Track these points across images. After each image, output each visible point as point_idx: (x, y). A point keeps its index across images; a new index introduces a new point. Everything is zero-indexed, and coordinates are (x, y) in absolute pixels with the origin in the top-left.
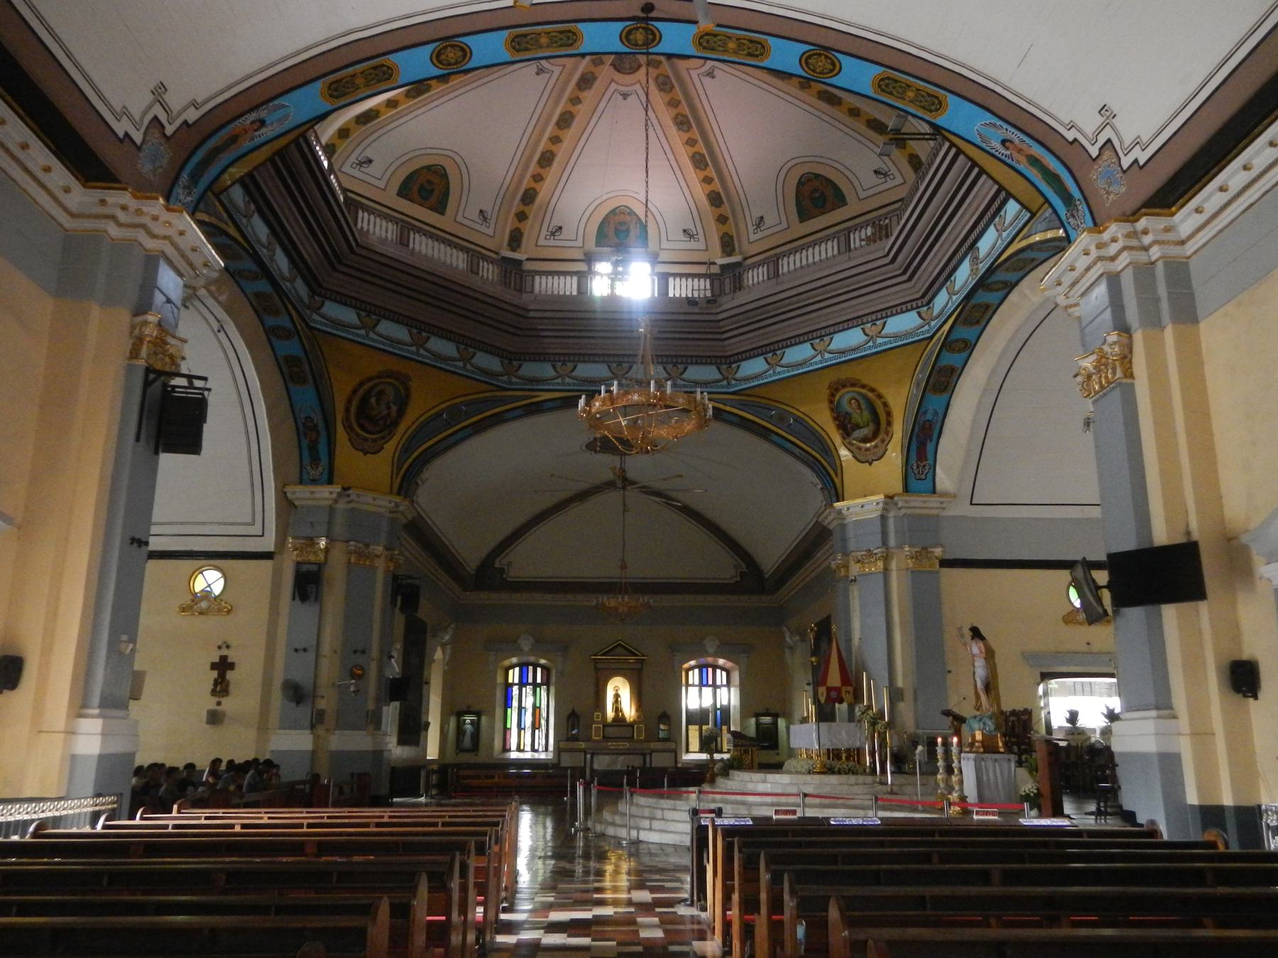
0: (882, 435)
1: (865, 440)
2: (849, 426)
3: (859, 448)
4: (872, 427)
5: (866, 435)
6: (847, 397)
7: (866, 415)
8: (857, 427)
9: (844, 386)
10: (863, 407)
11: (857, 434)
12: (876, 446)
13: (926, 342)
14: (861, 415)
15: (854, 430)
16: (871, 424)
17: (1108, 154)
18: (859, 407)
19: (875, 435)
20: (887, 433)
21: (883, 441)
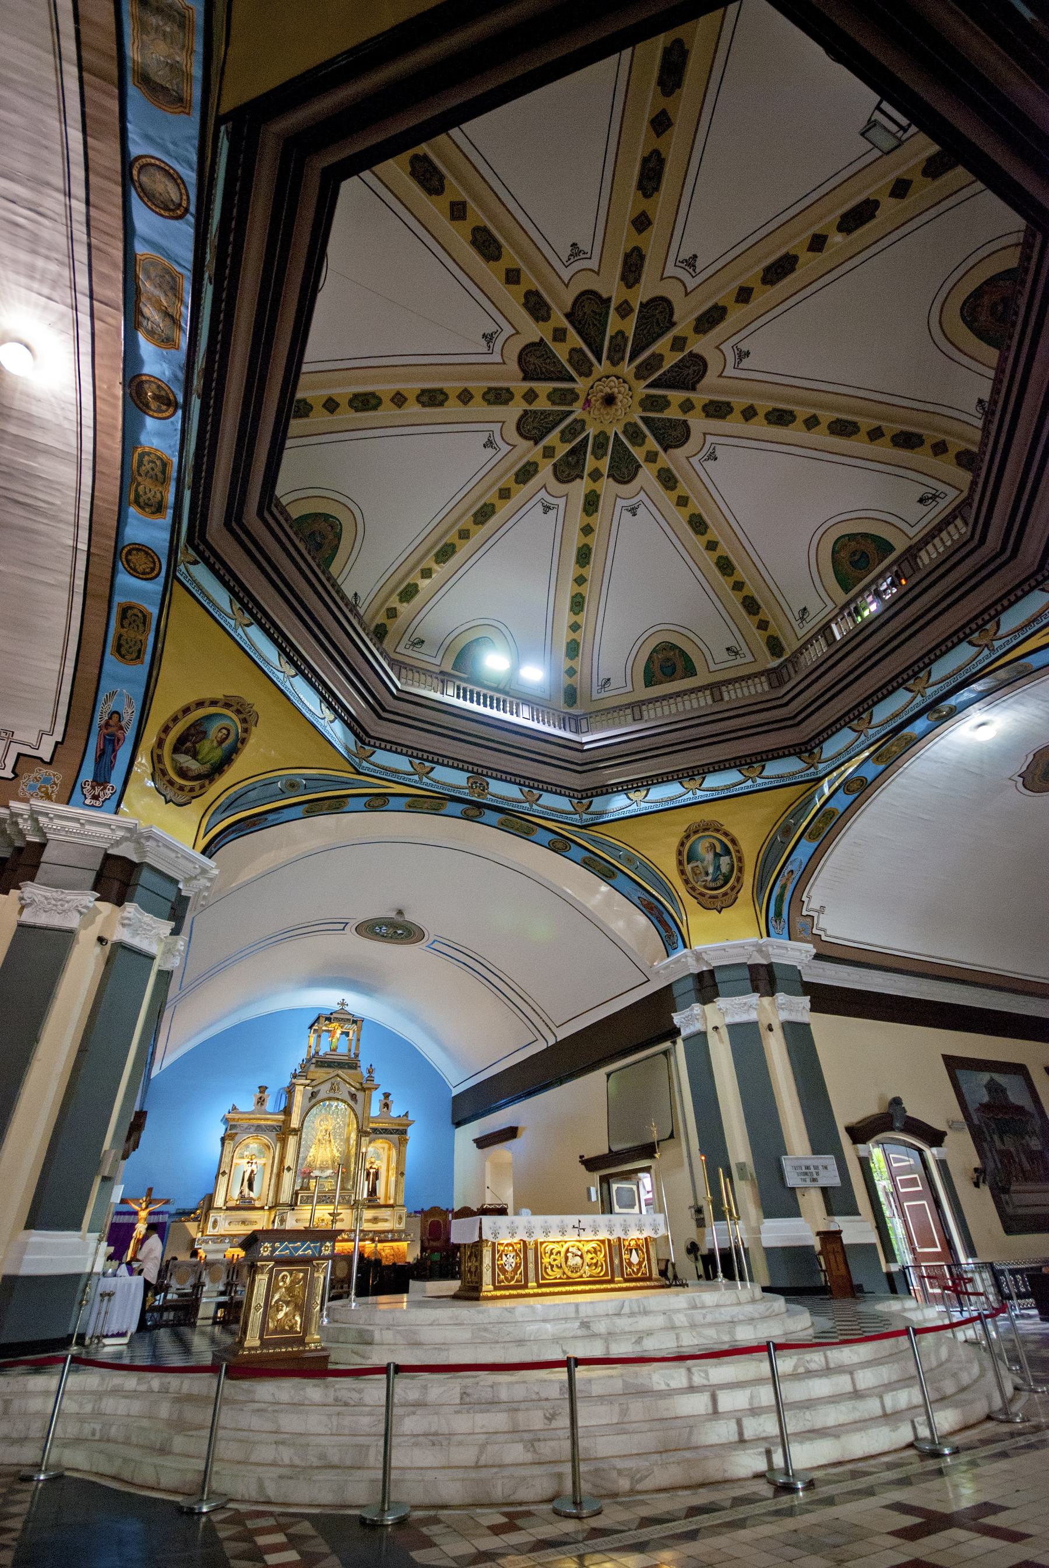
0: (196, 784)
1: (182, 773)
2: (189, 744)
3: (164, 773)
4: (204, 769)
5: (189, 769)
6: (224, 723)
7: (217, 754)
8: (195, 755)
9: (238, 712)
10: (225, 745)
11: (186, 761)
12: (181, 788)
13: (353, 770)
14: (213, 749)
15: (186, 753)
16: (208, 766)
17: (809, 919)
18: (221, 742)
19: (198, 777)
20: (202, 787)
21: (192, 790)
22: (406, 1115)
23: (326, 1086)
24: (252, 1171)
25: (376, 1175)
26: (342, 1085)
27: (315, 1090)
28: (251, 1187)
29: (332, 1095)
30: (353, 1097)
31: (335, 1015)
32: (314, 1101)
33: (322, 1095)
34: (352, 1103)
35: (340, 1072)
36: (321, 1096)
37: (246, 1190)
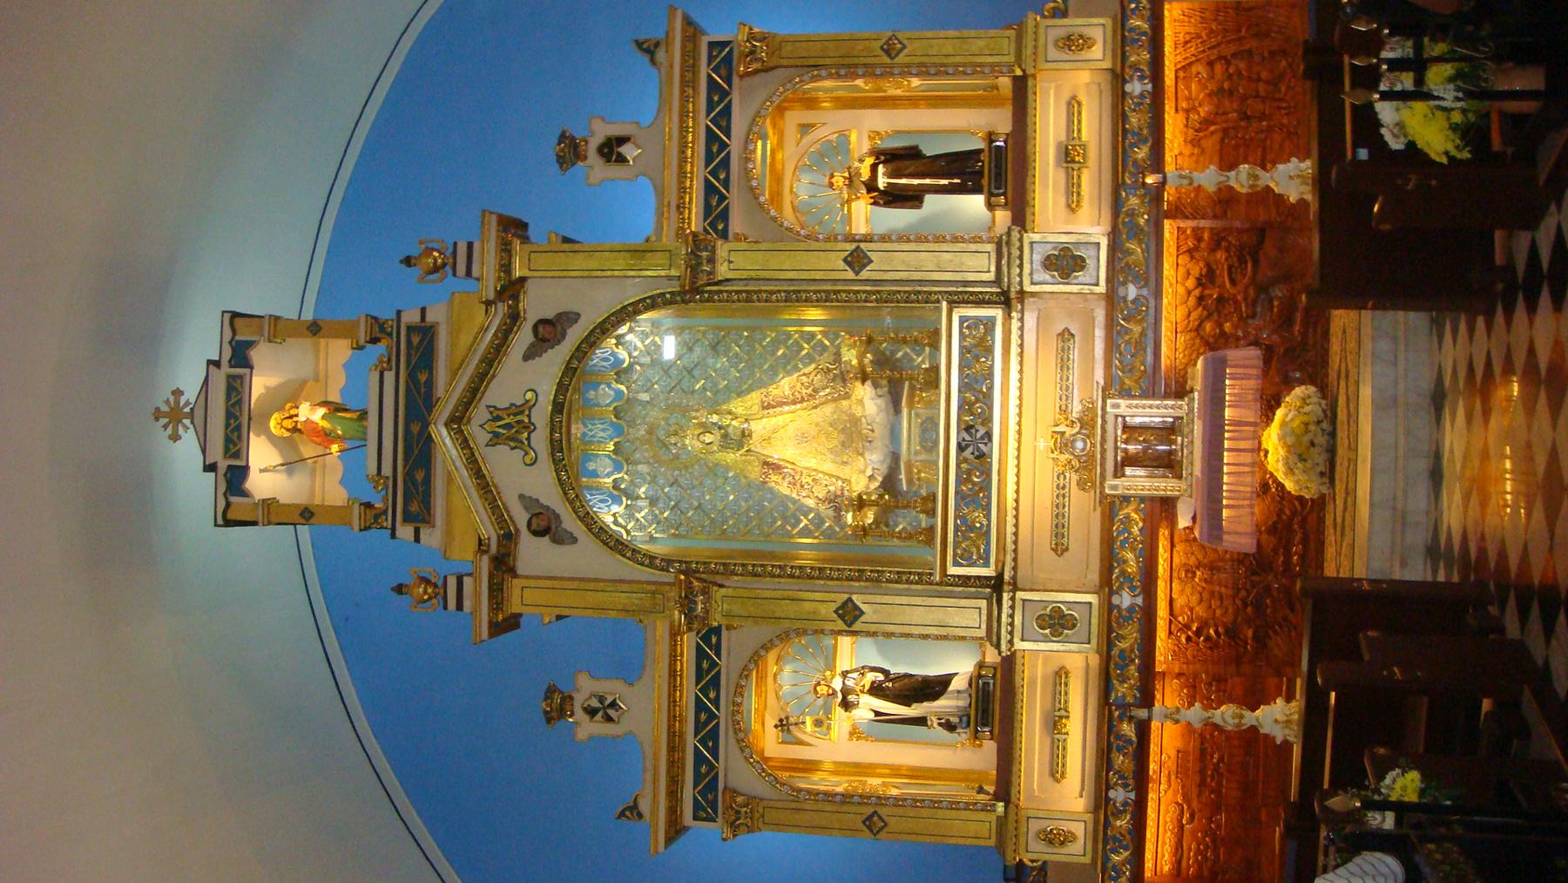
22: (649, 49)
23: (505, 466)
24: (876, 690)
25: (900, 158)
26: (504, 390)
27: (521, 517)
28: (933, 688)
29: (540, 439)
30: (549, 331)
31: (217, 453)
32: (570, 522)
33: (542, 484)
34: (575, 335)
35: (444, 411)
36: (550, 496)
37: (943, 703)
